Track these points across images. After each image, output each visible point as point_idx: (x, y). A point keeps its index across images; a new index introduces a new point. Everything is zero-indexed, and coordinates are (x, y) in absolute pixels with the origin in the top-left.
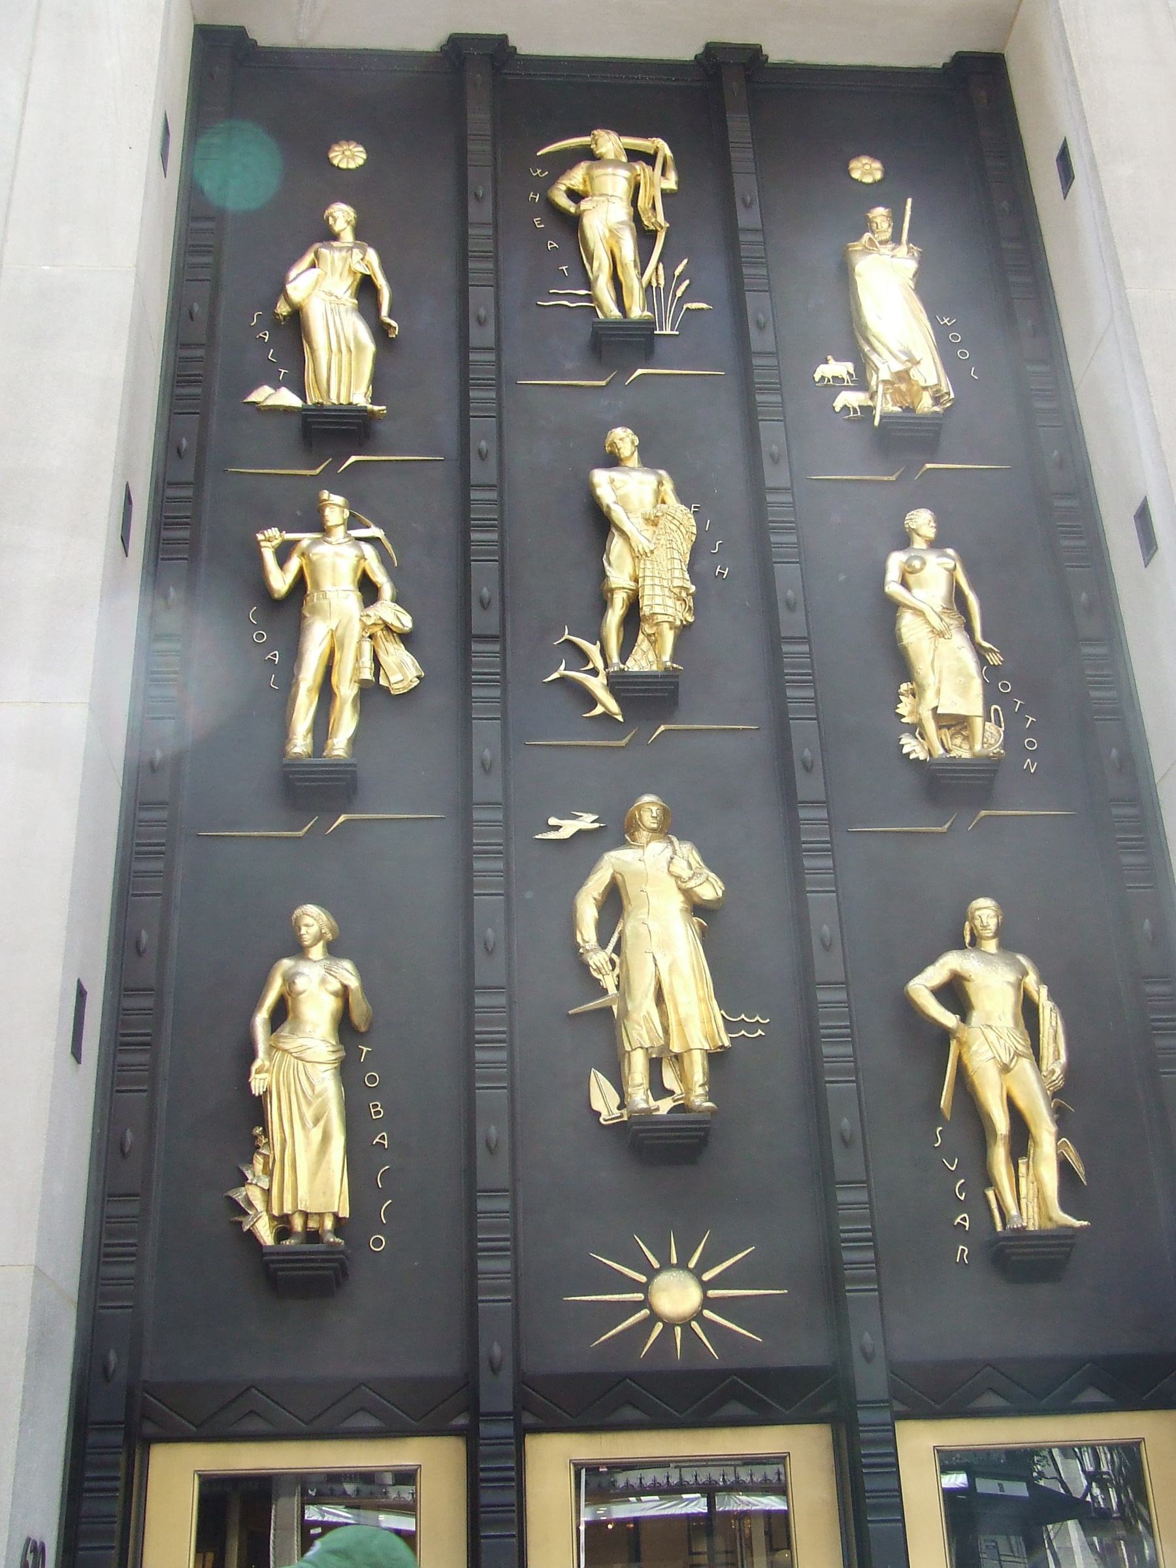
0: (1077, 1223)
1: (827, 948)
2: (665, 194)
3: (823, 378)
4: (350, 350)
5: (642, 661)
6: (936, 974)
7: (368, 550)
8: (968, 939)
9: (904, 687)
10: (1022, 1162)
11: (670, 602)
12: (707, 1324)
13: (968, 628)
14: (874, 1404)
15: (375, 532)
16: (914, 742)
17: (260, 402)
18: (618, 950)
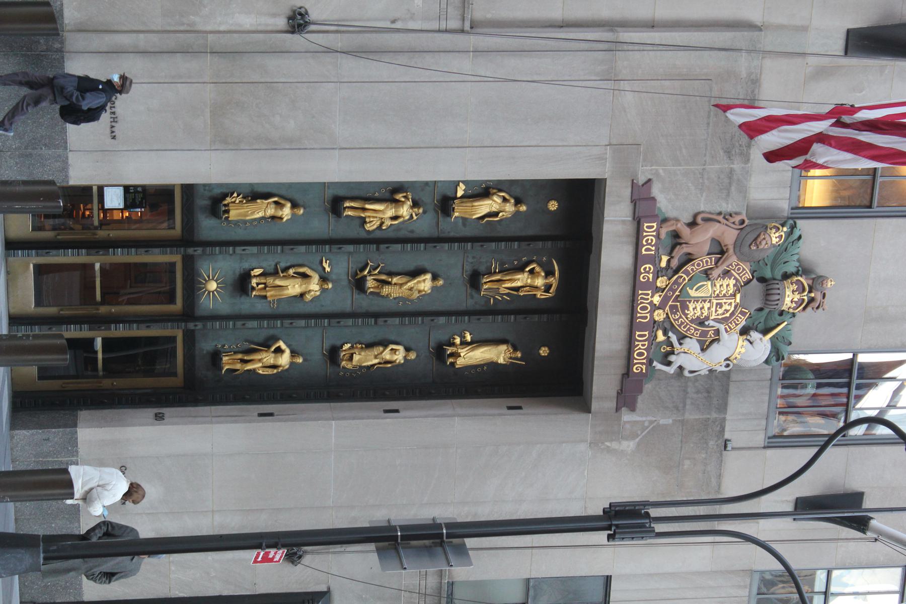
0: (223, 371)
1: (291, 323)
2: (535, 295)
3: (465, 333)
4: (472, 212)
5: (370, 283)
6: (283, 346)
7: (407, 218)
8: (293, 354)
9: (364, 346)
10: (239, 361)
11: (387, 292)
12: (205, 292)
13: (380, 363)
14: (186, 326)
15: (415, 218)
16: (348, 347)
17: (459, 186)
18: (292, 276)
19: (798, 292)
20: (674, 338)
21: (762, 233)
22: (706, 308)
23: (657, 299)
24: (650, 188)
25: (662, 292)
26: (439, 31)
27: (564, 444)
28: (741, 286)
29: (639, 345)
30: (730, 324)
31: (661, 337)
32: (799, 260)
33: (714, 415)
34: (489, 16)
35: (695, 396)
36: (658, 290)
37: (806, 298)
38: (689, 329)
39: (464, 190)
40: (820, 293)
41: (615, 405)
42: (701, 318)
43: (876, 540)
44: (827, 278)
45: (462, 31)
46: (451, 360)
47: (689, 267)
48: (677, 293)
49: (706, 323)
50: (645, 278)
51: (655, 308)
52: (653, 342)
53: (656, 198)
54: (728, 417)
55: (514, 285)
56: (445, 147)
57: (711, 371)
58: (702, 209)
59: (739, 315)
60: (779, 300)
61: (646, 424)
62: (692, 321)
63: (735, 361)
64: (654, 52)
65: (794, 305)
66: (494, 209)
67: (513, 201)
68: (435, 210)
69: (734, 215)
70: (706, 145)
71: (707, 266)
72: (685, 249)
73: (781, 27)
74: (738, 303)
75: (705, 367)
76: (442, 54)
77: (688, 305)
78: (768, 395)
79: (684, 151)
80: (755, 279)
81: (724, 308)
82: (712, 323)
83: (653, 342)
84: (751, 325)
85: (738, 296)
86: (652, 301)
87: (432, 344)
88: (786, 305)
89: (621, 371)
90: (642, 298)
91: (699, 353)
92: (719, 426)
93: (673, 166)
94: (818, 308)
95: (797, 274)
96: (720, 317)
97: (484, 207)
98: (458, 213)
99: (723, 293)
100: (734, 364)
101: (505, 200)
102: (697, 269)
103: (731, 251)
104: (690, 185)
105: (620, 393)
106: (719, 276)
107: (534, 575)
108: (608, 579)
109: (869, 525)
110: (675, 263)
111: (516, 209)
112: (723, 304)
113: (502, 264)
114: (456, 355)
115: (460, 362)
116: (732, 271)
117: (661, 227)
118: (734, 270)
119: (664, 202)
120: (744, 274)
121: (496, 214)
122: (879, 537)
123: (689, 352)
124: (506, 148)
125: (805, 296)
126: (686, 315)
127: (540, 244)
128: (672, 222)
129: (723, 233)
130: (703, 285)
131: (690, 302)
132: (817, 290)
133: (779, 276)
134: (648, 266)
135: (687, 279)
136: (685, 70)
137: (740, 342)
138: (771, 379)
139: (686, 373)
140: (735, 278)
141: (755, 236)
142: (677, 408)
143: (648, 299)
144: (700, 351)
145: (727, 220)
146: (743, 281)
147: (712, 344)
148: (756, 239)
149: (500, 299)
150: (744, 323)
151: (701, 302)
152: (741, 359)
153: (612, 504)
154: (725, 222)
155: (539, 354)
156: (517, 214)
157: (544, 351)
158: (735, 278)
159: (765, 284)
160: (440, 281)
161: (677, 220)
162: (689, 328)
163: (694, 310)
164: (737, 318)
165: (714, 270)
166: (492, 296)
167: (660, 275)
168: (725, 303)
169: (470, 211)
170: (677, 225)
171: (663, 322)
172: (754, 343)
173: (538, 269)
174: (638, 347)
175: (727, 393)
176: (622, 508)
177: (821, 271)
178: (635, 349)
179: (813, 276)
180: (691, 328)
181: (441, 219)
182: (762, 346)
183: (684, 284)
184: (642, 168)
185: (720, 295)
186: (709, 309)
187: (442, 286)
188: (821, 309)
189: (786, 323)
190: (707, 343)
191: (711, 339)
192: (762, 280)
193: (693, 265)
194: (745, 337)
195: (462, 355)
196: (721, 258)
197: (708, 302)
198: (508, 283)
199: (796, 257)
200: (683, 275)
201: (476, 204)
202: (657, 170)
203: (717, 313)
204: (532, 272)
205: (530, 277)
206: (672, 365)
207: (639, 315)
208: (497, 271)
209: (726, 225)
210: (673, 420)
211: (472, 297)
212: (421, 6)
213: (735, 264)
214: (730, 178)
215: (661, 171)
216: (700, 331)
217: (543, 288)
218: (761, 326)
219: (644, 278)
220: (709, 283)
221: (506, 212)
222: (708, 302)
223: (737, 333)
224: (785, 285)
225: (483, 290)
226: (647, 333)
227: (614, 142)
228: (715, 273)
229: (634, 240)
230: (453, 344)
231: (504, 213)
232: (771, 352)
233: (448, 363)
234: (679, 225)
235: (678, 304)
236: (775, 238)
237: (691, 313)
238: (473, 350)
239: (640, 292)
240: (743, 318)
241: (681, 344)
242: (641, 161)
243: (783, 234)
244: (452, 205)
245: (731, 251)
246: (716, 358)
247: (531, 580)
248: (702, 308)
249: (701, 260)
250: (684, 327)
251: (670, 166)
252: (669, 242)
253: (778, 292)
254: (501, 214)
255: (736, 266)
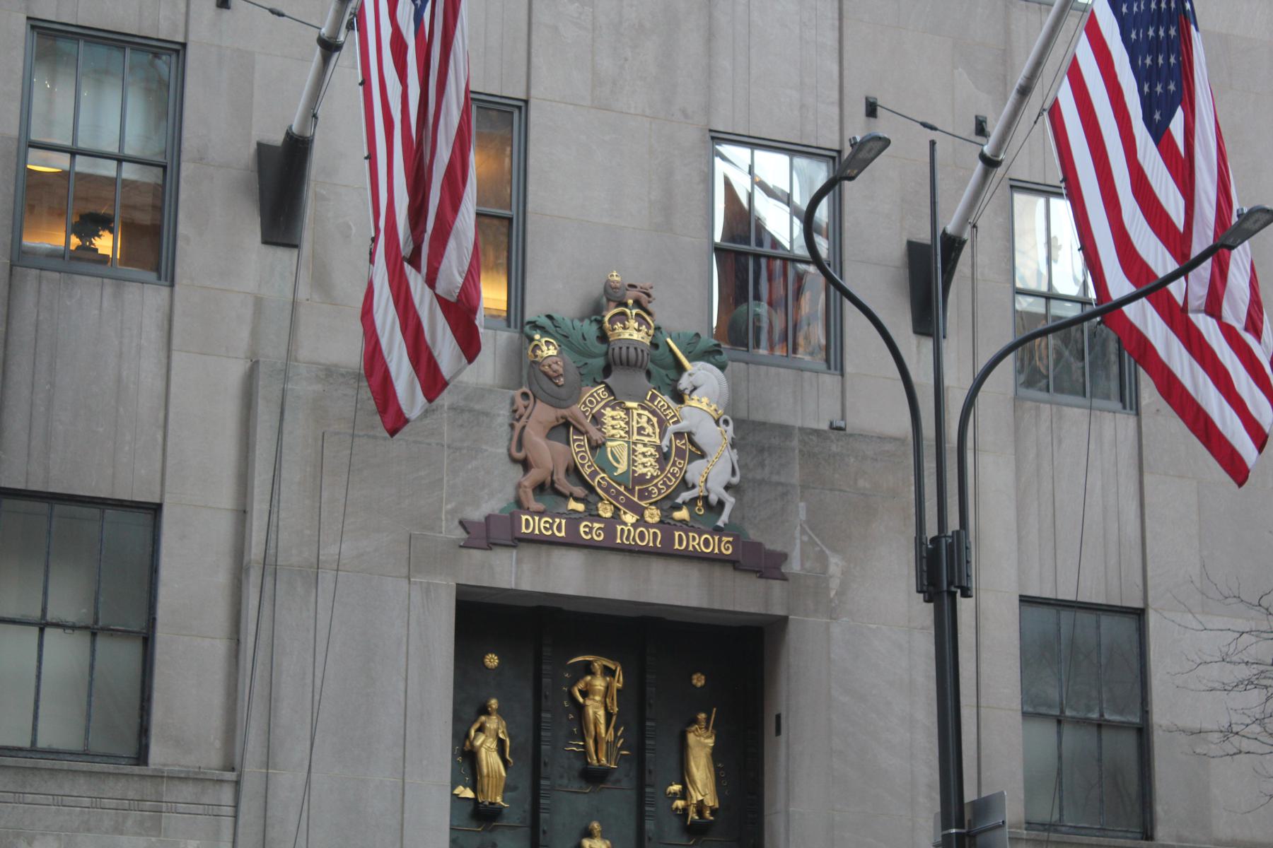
4: (496, 776)
17: (458, 795)
19: (626, 323)
20: (686, 496)
21: (543, 369)
22: (645, 450)
23: (630, 518)
24: (473, 523)
25: (619, 509)
26: (236, 817)
27: (832, 656)
28: (615, 399)
29: (693, 546)
30: (668, 418)
31: (683, 514)
32: (582, 320)
33: (795, 443)
34: (218, 744)
35: (767, 470)
36: (616, 516)
37: (634, 312)
38: (673, 475)
39: (465, 787)
40: (628, 292)
41: (778, 582)
42: (658, 456)
43: (974, 226)
44: (608, 281)
45: (237, 783)
46: (707, 814)
47: (586, 472)
48: (622, 489)
49: (665, 449)
50: (599, 533)
51: (641, 522)
52: (690, 524)
53: (486, 514)
54: (798, 424)
55: (602, 720)
56: (403, 813)
57: (733, 445)
58: (504, 451)
59: (656, 403)
60: (636, 349)
61: (805, 538)
62: (662, 469)
63: (720, 412)
64: (280, 512)
65: (644, 328)
66: (494, 745)
67: (483, 718)
68: (491, 831)
69: (515, 407)
70: (415, 442)
71: (584, 446)
72: (560, 477)
73: (255, 334)
74: (639, 405)
75: (726, 453)
76: (269, 814)
77: (639, 475)
78: (769, 368)
79: (422, 473)
80: (606, 381)
81: (645, 425)
82: (665, 442)
83: (690, 524)
84: (671, 388)
85: (629, 404)
86: (633, 525)
87: (683, 841)
88: (642, 338)
89: (729, 572)
90: (628, 539)
91: (708, 461)
92: (811, 437)
93: (442, 489)
94: (649, 295)
95: (600, 323)
96: (657, 430)
97: (490, 760)
98: (498, 798)
99: (624, 425)
100: (724, 414)
101: (481, 729)
102: (589, 460)
103: (565, 412)
104: (470, 467)
105: (761, 574)
106: (600, 430)
107: (1016, 704)
108: (1025, 600)
109: (952, 236)
110: (580, 491)
111: (495, 713)
112: (639, 425)
113: (572, 736)
114: (700, 806)
115: (711, 801)
116: (594, 411)
117: (528, 509)
118: (592, 409)
119: (492, 504)
120: (598, 395)
121: (501, 743)
122: (970, 223)
123: (705, 475)
124: (408, 725)
125: (631, 313)
126: (653, 478)
127: (546, 681)
128: (522, 494)
129: (540, 423)
130: (612, 453)
131: (634, 471)
132: (624, 295)
133: (602, 348)
134: (582, 529)
135: (603, 475)
136: (308, 469)
137: (694, 403)
138: (747, 363)
139: (736, 480)
140: (604, 407)
141: (546, 379)
142: (784, 495)
143: (629, 530)
144: (705, 460)
145: (521, 417)
146: (608, 397)
147: (696, 443)
148: (550, 378)
149: (621, 741)
150: (666, 398)
151: (636, 456)
152: (717, 403)
153: (919, 589)
154: (524, 419)
155: (702, 687)
156: (501, 712)
157: (698, 680)
158: (604, 407)
159: (613, 368)
160: (593, 826)
161: (519, 486)
162: (671, 474)
163: (646, 466)
164: (659, 407)
165: (592, 438)
166: (618, 753)
167: (594, 513)
168: (638, 422)
169: (495, 780)
170: (525, 487)
171: (662, 510)
172: (696, 384)
173: (581, 685)
174: (697, 547)
175: (764, 424)
176: (925, 575)
177: (597, 290)
178: (699, 550)
179: (604, 300)
180: (671, 471)
181: (505, 823)
182: (700, 374)
183: (608, 479)
184: (444, 532)
185: (627, 429)
186: (645, 445)
187: (601, 823)
188: (650, 291)
189: (669, 340)
190: (694, 449)
191: (688, 443)
192: (607, 371)
193: (583, 465)
194: (687, 397)
195: (700, 798)
196: (575, 428)
197: (636, 446)
198: (600, 728)
199: (577, 323)
200: (597, 480)
201: (485, 771)
202: (447, 512)
203: (651, 434)
204: (585, 694)
205: (591, 697)
206: (724, 500)
207: (651, 544)
208: (581, 743)
209: (528, 418)
210: (801, 501)
211: (618, 781)
212: (198, 842)
213: (584, 408)
214: (462, 411)
215: (449, 507)
216: (676, 459)
217: (608, 679)
218: (672, 374)
219: (599, 535)
220: (609, 444)
221: (499, 728)
222: (636, 446)
223: (681, 408)
224: (616, 340)
225: (608, 765)
226: (677, 534)
227: (404, 571)
228: (596, 435)
229: (544, 547)
230: (685, 810)
231: (500, 731)
232: (709, 361)
233: (712, 818)
234: (526, 483)
235: (637, 488)
236: (549, 351)
237: (650, 471)
238: (693, 782)
239: (619, 541)
240: (659, 399)
241: (694, 486)
242: (432, 534)
243: (543, 340)
244: (485, 805)
245: (565, 412)
246: (715, 437)
247: (1025, 709)
248: (644, 454)
249: (577, 454)
250: (670, 480)
251: (442, 494)
252: (550, 498)
253: (624, 349)
254: (501, 736)
255: (586, 406)
